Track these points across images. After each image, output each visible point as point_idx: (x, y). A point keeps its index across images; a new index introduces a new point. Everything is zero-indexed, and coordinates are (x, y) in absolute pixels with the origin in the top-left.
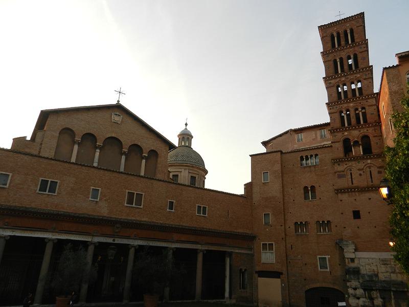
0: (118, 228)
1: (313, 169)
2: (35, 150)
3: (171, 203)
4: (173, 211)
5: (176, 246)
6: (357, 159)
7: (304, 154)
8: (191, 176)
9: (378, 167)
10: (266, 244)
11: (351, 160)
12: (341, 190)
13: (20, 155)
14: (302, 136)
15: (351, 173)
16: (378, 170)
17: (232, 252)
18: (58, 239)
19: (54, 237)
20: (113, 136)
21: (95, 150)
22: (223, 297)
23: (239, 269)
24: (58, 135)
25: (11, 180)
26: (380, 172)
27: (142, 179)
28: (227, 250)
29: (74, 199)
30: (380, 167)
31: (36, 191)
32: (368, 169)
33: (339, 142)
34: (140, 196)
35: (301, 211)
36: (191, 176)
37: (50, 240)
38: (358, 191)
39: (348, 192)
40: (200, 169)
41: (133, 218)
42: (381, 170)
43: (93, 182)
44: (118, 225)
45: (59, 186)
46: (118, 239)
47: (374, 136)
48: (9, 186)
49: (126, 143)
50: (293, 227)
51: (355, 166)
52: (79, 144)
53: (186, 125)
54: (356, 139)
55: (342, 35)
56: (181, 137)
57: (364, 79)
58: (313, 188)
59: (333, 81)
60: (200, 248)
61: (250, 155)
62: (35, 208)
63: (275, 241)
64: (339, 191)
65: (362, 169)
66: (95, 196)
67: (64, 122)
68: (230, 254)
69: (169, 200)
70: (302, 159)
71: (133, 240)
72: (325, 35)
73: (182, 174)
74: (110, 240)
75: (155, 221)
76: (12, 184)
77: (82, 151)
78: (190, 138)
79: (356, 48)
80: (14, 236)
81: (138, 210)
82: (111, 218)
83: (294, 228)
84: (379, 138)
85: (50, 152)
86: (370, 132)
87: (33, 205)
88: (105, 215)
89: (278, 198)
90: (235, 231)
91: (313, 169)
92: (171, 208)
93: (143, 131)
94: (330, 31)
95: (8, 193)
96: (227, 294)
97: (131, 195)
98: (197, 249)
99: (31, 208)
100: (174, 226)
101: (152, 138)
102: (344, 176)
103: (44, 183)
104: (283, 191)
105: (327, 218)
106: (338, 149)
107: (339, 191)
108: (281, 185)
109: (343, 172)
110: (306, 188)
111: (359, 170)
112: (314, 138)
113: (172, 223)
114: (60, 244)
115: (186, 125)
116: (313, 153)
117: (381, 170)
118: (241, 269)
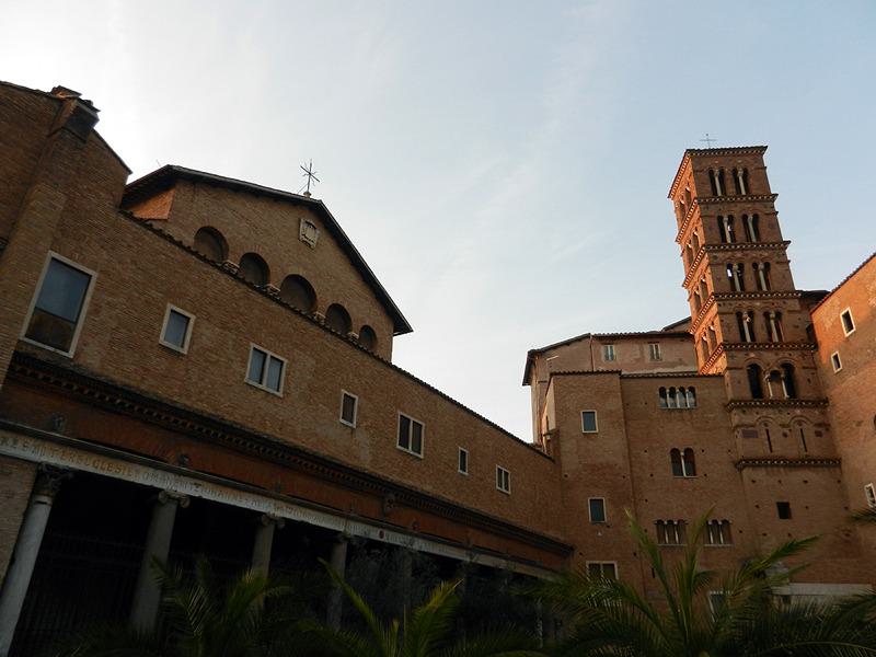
1: (686, 414)
6: (776, 404)
7: (668, 384)
9: (816, 425)
10: (599, 565)
11: (766, 407)
12: (754, 460)
14: (615, 349)
15: (767, 431)
16: (816, 429)
19: (279, 514)
25: (193, 333)
26: (819, 434)
29: (313, 414)
30: (819, 425)
31: (243, 377)
32: (798, 427)
33: (741, 369)
35: (668, 498)
37: (272, 520)
38: (784, 466)
39: (766, 466)
42: (820, 429)
45: (288, 374)
47: (804, 368)
49: (325, 299)
50: (653, 530)
51: (777, 418)
54: (776, 369)
55: (729, 177)
57: (778, 263)
58: (689, 452)
59: (720, 255)
63: (616, 559)
64: (742, 464)
65: (788, 426)
66: (348, 415)
67: (205, 210)
70: (662, 392)
72: (698, 168)
79: (758, 205)
80: (200, 498)
83: (655, 531)
84: (813, 371)
86: (795, 358)
89: (620, 468)
91: (686, 414)
93: (351, 277)
94: (707, 163)
95: (187, 370)
101: (366, 299)
102: (754, 435)
104: (629, 453)
105: (721, 516)
106: (739, 382)
107: (742, 464)
108: (625, 442)
109: (753, 426)
110: (675, 452)
111: (783, 426)
112: (638, 357)
114: (290, 532)
116: (686, 383)
117: (820, 429)
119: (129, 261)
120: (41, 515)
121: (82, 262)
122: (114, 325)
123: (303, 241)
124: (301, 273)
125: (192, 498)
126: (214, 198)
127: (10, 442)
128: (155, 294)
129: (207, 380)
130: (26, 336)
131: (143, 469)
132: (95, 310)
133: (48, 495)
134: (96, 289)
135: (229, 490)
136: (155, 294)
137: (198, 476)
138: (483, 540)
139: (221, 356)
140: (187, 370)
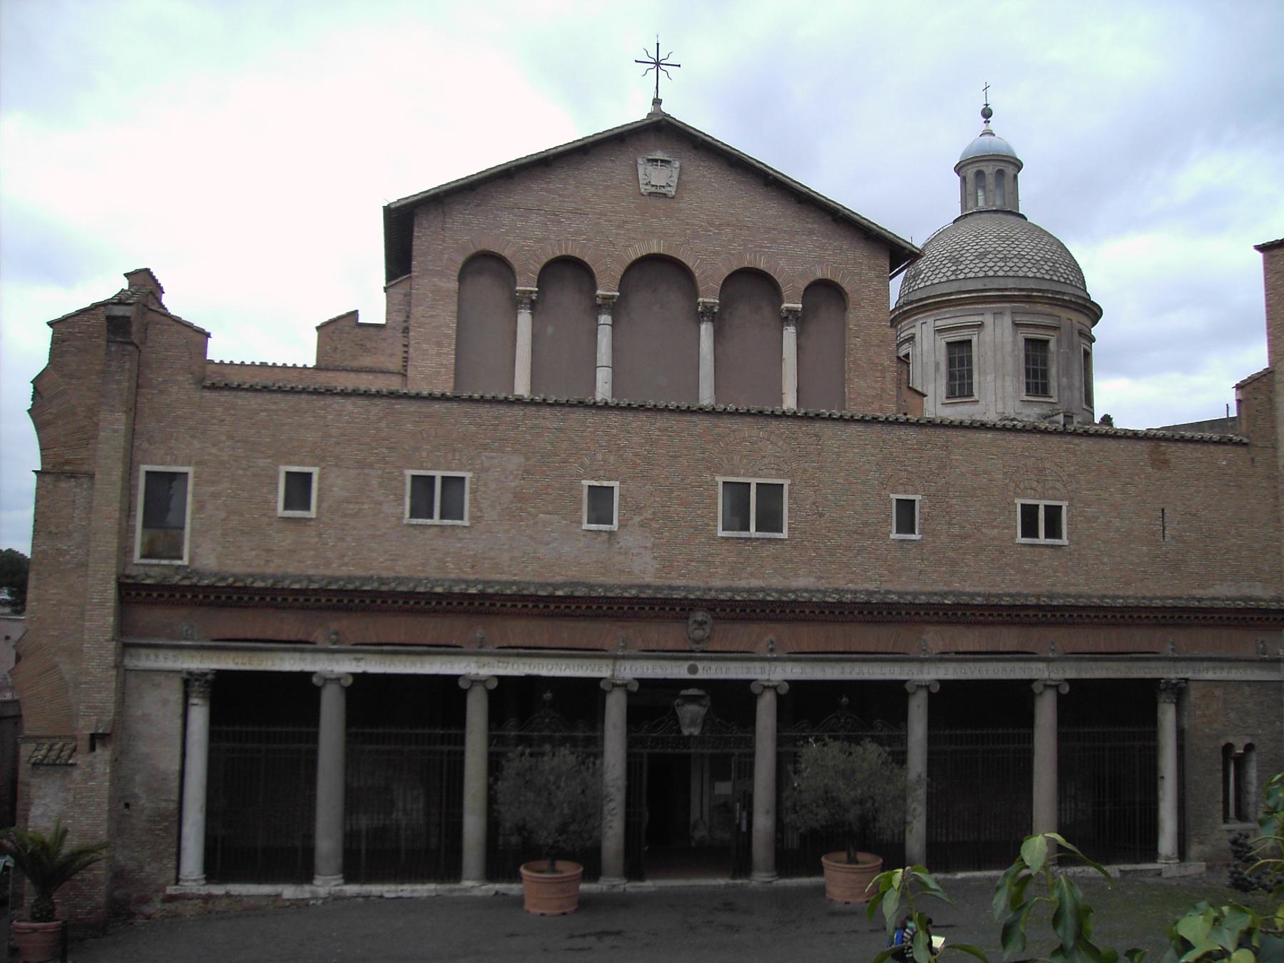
0: (701, 624)
2: (392, 355)
3: (906, 508)
4: (916, 537)
5: (942, 676)
8: (1027, 340)
13: (329, 400)
17: (1187, 680)
18: (498, 677)
20: (655, 250)
21: (597, 320)
22: (1151, 852)
23: (1223, 744)
24: (454, 285)
25: (320, 489)
27: (774, 423)
28: (1165, 676)
31: (401, 518)
34: (770, 494)
36: (1027, 340)
37: (475, 681)
40: (1066, 305)
41: (755, 583)
43: (587, 461)
44: (700, 616)
45: (473, 491)
46: (706, 664)
48: (318, 513)
52: (533, 306)
53: (987, 114)
56: (970, 172)
60: (1045, 675)
61: (1259, 248)
62: (409, 579)
68: (1179, 691)
69: (894, 497)
71: (766, 665)
73: (987, 334)
74: (678, 671)
75: (841, 584)
76: (325, 505)
77: (550, 330)
78: (1010, 170)
80: (364, 675)
81: (771, 549)
82: (671, 588)
85: (439, 355)
87: (401, 569)
88: (648, 579)
90: (1198, 592)
92: (906, 524)
93: (772, 210)
95: (320, 535)
96: (1167, 842)
97: (737, 492)
98: (1032, 681)
99: (396, 578)
100: (923, 599)
101: (811, 232)
103: (423, 485)
113: (915, 587)
115: (987, 114)
118: (1228, 748)
119: (224, 438)
120: (199, 716)
121: (175, 462)
122: (223, 515)
123: (650, 194)
124: (655, 247)
125: (355, 675)
126: (478, 205)
127: (153, 657)
128: (262, 462)
129: (349, 539)
130: (143, 557)
131: (287, 656)
132: (200, 506)
133: (196, 697)
134: (196, 485)
135: (403, 658)
136: (262, 462)
137: (361, 648)
138: (971, 639)
139: (363, 503)
140: (320, 535)
